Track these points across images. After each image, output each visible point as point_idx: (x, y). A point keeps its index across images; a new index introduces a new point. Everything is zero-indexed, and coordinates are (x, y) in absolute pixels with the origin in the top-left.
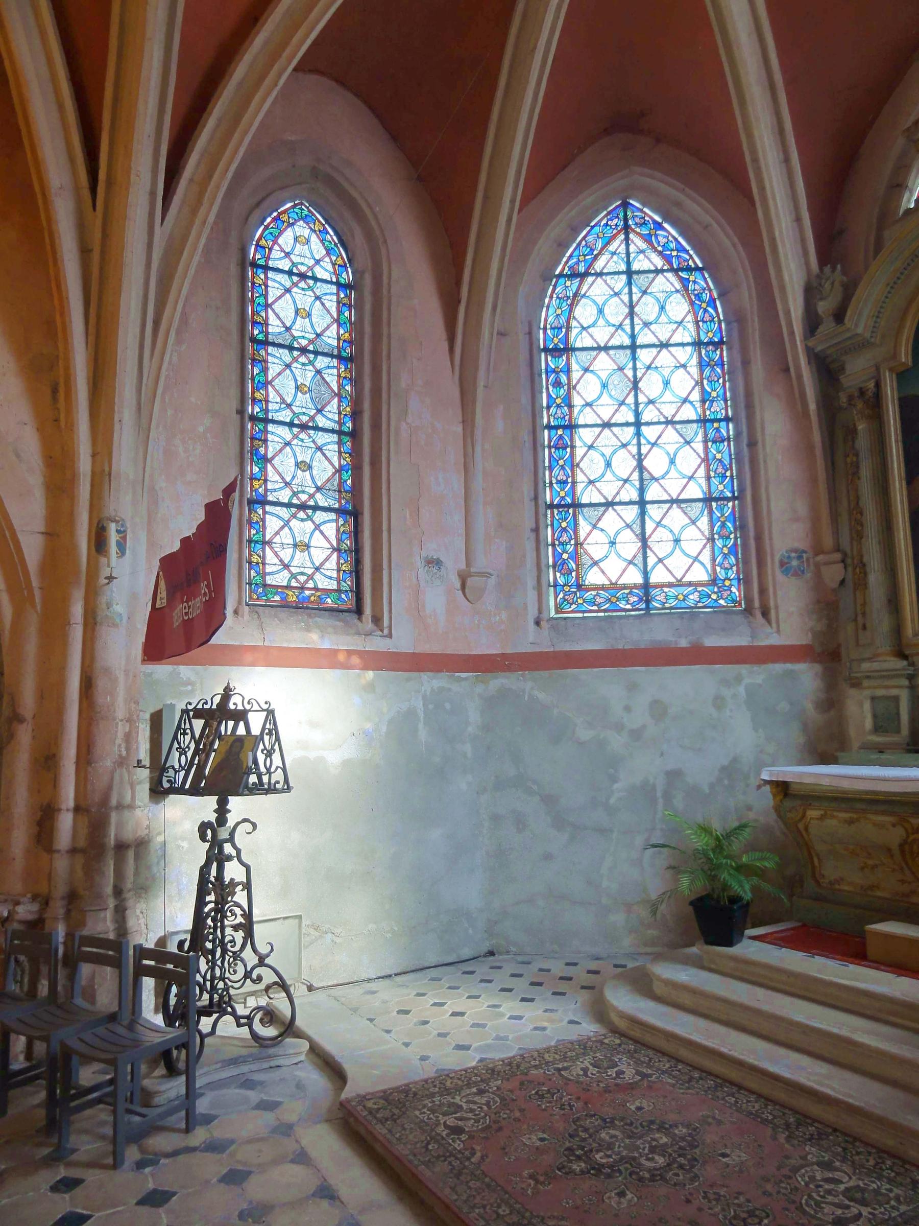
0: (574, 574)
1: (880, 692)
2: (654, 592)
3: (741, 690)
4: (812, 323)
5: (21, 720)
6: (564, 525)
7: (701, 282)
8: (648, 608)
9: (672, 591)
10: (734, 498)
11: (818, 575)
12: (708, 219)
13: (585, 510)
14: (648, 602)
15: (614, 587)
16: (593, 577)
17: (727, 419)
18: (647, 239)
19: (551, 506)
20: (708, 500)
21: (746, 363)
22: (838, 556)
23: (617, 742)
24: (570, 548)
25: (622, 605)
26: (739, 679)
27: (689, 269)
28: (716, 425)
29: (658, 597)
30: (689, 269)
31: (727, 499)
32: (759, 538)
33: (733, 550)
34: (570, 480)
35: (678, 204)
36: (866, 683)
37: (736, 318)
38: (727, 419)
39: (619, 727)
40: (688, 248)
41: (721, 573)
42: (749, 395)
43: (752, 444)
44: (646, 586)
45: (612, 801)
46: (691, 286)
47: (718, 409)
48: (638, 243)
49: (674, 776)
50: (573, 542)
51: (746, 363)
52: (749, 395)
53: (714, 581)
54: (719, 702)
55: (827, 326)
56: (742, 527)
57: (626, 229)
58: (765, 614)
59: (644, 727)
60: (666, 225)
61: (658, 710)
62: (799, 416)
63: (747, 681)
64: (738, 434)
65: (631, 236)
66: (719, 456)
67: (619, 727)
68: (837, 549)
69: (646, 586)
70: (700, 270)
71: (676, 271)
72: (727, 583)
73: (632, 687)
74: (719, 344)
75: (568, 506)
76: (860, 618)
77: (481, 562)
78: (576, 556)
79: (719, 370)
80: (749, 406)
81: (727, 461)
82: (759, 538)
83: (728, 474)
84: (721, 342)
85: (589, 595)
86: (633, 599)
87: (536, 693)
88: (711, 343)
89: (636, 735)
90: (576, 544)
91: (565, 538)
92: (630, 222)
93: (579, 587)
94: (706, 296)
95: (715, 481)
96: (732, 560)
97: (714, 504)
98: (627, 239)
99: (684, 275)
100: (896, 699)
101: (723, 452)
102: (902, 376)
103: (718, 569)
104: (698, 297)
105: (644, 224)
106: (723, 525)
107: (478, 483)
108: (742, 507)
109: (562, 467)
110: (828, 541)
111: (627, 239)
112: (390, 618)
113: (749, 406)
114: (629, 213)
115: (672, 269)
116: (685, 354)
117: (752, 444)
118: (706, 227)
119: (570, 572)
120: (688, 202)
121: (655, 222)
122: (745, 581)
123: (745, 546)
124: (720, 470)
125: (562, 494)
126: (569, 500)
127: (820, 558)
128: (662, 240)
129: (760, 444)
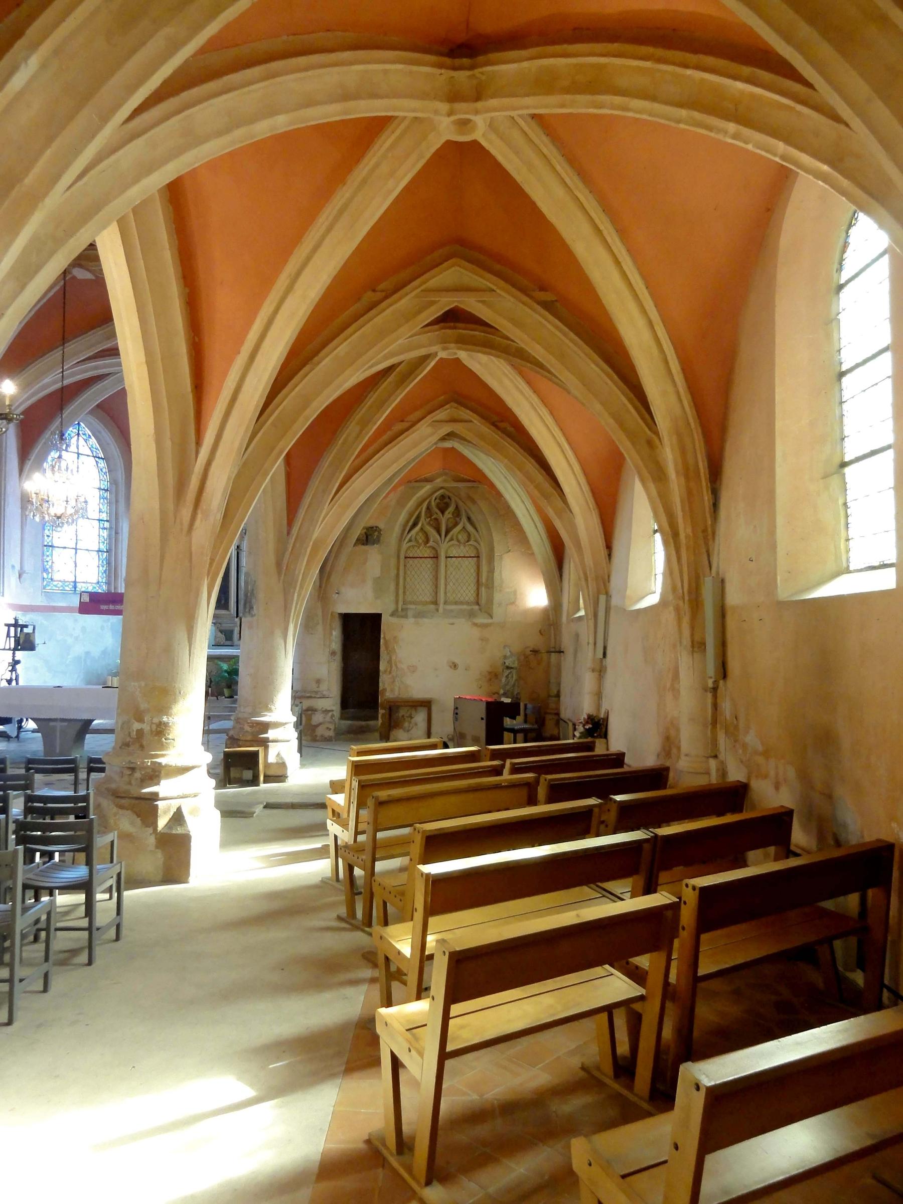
0: (50, 574)
2: (77, 584)
3: (110, 624)
6: (48, 553)
7: (102, 464)
8: (75, 590)
10: (107, 552)
12: (110, 442)
13: (56, 549)
14: (75, 588)
16: (55, 577)
17: (107, 521)
18: (86, 441)
19: (46, 546)
20: (99, 551)
21: (117, 501)
23: (70, 641)
24: (50, 563)
25: (67, 588)
26: (108, 620)
27: (99, 458)
28: (103, 522)
30: (99, 458)
31: (105, 552)
32: (115, 569)
33: (105, 572)
34: (51, 536)
35: (100, 432)
37: (114, 482)
38: (107, 521)
39: (71, 635)
40: (100, 449)
41: (100, 580)
43: (116, 533)
44: (75, 582)
45: (68, 662)
46: (99, 465)
47: (104, 516)
48: (82, 442)
49: (87, 653)
50: (51, 561)
51: (117, 501)
53: (98, 583)
54: (102, 628)
56: (109, 564)
57: (78, 434)
59: (79, 635)
60: (92, 437)
61: (84, 629)
63: (111, 621)
64: (111, 528)
65: (80, 438)
66: (103, 535)
67: (71, 635)
70: (103, 459)
71: (94, 457)
72: (102, 584)
73: (76, 620)
75: (50, 546)
77: (27, 568)
78: (51, 567)
79: (106, 501)
80: (117, 519)
81: (106, 537)
83: (106, 542)
84: (107, 490)
85: (55, 583)
86: (71, 586)
87: (43, 621)
88: (104, 489)
89: (77, 638)
90: (52, 562)
91: (48, 559)
92: (80, 432)
93: (52, 579)
94: (104, 470)
95: (101, 544)
96: (105, 575)
97: (100, 553)
98: (78, 439)
99: (97, 459)
101: (105, 534)
103: (100, 578)
104: (101, 470)
105: (84, 434)
106: (103, 562)
107: (26, 536)
108: (110, 556)
109: (49, 530)
111: (78, 439)
112: (3, 589)
113: (117, 519)
114: (80, 429)
115: (93, 456)
117: (116, 533)
118: (108, 444)
119: (49, 573)
120: (103, 433)
121: (89, 435)
124: (103, 540)
125: (48, 541)
126: (50, 544)
128: (91, 443)
129: (120, 534)
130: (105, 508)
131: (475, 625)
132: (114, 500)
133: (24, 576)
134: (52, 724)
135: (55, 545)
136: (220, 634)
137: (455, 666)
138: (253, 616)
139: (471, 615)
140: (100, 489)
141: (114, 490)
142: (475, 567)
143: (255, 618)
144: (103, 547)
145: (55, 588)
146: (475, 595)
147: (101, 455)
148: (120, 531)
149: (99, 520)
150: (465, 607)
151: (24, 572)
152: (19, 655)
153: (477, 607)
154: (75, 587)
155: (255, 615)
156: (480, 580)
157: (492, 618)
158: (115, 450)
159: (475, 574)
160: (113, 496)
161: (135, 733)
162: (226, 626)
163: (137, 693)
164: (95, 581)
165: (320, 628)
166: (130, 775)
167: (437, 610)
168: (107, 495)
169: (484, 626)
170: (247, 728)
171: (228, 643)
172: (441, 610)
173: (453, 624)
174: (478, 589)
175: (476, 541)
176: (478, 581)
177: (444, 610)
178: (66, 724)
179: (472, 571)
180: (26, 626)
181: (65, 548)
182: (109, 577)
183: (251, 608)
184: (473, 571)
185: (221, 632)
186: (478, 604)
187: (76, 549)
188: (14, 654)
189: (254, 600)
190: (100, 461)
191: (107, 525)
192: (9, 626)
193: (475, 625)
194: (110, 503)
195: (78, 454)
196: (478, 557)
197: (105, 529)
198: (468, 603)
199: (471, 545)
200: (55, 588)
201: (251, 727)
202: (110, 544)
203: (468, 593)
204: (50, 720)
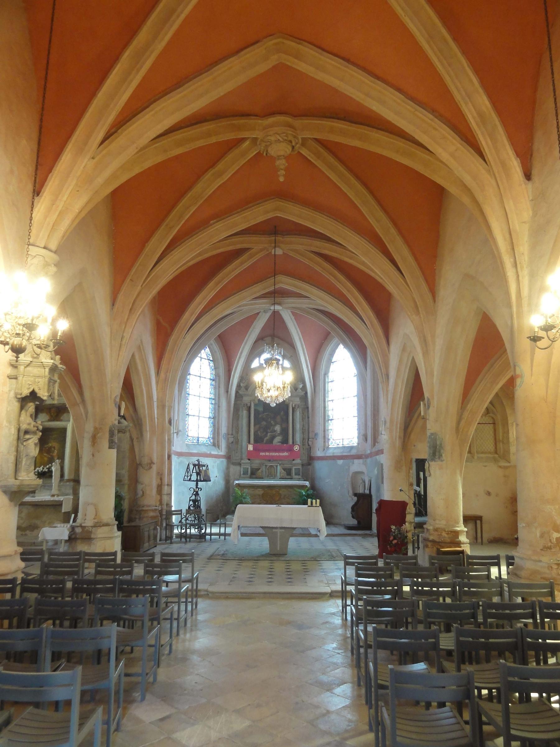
1: (245, 467)
2: (199, 439)
4: (239, 386)
5: (154, 464)
7: (212, 364)
8: (198, 443)
9: (202, 439)
10: (213, 418)
11: (228, 439)
12: (217, 351)
15: (193, 437)
16: (190, 435)
17: (213, 399)
20: (209, 418)
21: (219, 387)
22: (233, 436)
25: (195, 441)
29: (200, 439)
36: (242, 465)
37: (217, 375)
38: (213, 399)
42: (219, 395)
43: (219, 407)
44: (198, 438)
47: (212, 396)
51: (219, 387)
52: (219, 395)
53: (209, 438)
55: (243, 389)
56: (214, 426)
58: (218, 447)
62: (229, 402)
64: (215, 404)
68: (232, 435)
69: (198, 438)
71: (208, 360)
74: (213, 380)
76: (236, 451)
80: (219, 398)
82: (218, 429)
85: (189, 438)
88: (212, 380)
100: (248, 468)
101: (212, 406)
102: (255, 405)
110: (230, 433)
113: (219, 398)
116: (209, 382)
122: (213, 438)
123: (214, 430)
127: (230, 436)
130: (213, 391)
131: (500, 467)
132: (217, 385)
133: (180, 433)
134: (274, 530)
135: (189, 414)
136: (283, 471)
137: (489, 494)
138: (442, 461)
139: (495, 460)
140: (210, 379)
141: (217, 380)
142: (493, 430)
143: (444, 462)
144: (211, 415)
145: (189, 441)
146: (494, 448)
147: (211, 359)
148: (220, 405)
149: (210, 399)
150: (490, 455)
151: (180, 431)
152: (200, 484)
153: (496, 456)
154: (198, 440)
155: (444, 460)
156: (497, 438)
157: (510, 463)
158: (219, 355)
159: (493, 435)
160: (217, 384)
161: (555, 540)
162: (287, 466)
163: (553, 513)
164: (207, 437)
165: (404, 468)
166: (557, 569)
167: (473, 457)
168: (214, 383)
169: (506, 468)
170: (444, 534)
171: (289, 477)
172: (476, 457)
173: (486, 466)
174: (496, 444)
175: (494, 413)
176: (495, 439)
177: (478, 457)
178: (283, 530)
179: (491, 432)
180: (204, 466)
181: (194, 416)
182: (214, 434)
183: (440, 456)
184: (492, 433)
185: (284, 469)
186: (496, 452)
187: (199, 416)
188: (197, 484)
189: (442, 451)
190: (211, 362)
191: (213, 402)
192: (195, 465)
193: (500, 467)
194: (215, 388)
195: (201, 358)
196: (494, 424)
197: (212, 404)
198: (490, 453)
199: (490, 416)
200: (189, 441)
201: (448, 534)
202: (215, 413)
203: (490, 446)
204: (273, 528)
